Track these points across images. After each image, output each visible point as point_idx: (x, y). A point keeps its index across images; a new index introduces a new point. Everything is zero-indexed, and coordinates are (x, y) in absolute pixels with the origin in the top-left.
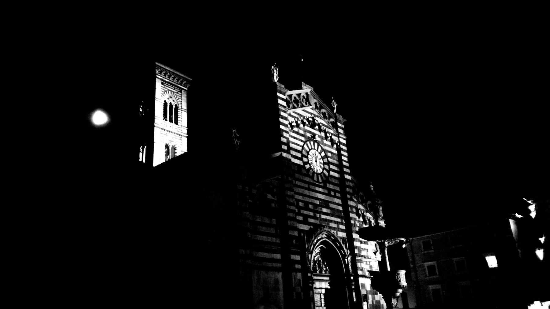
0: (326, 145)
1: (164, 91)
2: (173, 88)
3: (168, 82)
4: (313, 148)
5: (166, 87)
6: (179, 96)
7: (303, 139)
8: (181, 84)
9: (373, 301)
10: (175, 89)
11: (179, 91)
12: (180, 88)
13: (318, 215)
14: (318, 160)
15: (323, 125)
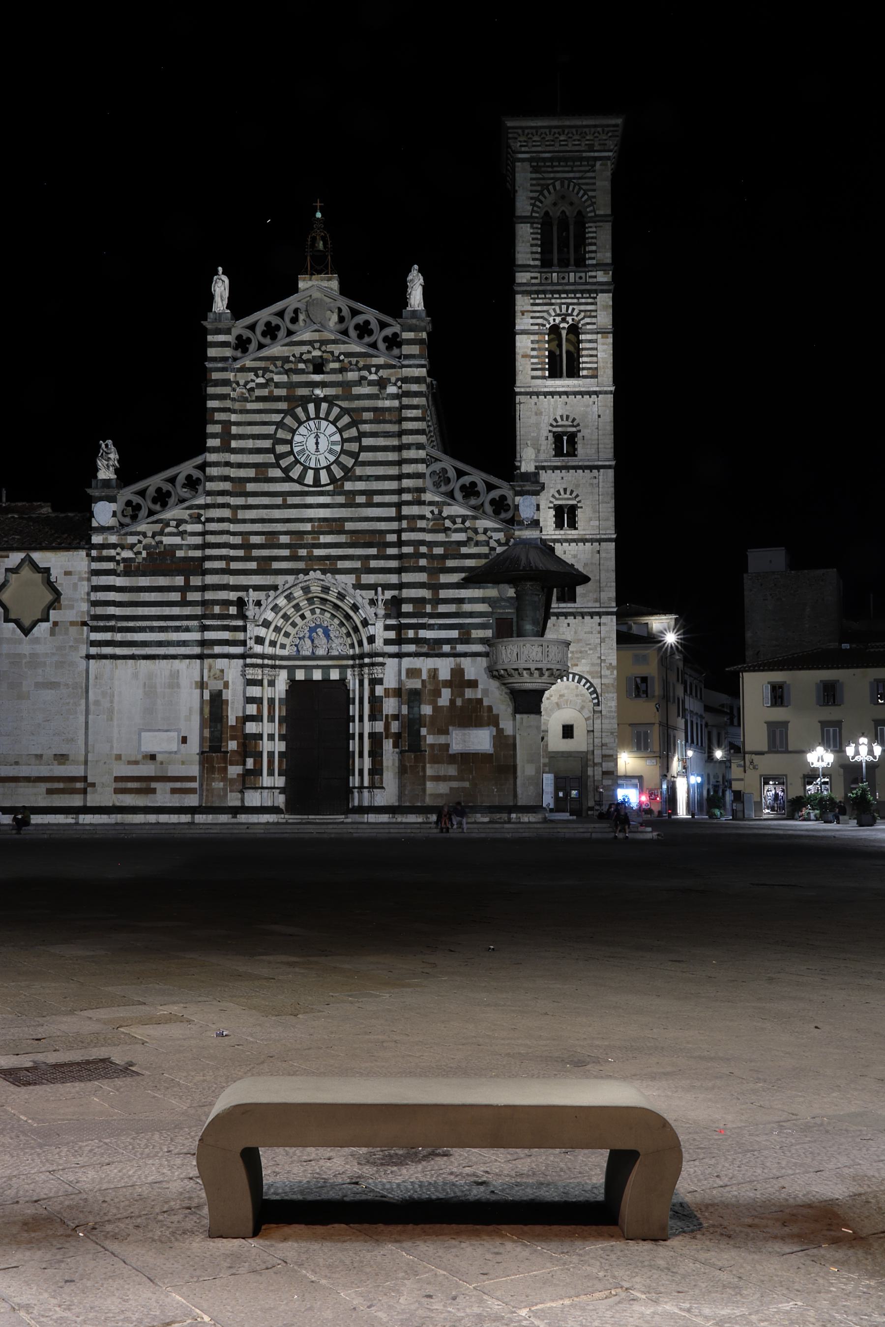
0: (360, 397)
1: (539, 188)
2: (566, 169)
3: (551, 159)
4: (312, 414)
5: (546, 175)
6: (587, 184)
7: (283, 406)
8: (591, 149)
9: (452, 701)
10: (575, 169)
11: (587, 168)
12: (588, 159)
13: (303, 552)
14: (323, 442)
15: (348, 355)
